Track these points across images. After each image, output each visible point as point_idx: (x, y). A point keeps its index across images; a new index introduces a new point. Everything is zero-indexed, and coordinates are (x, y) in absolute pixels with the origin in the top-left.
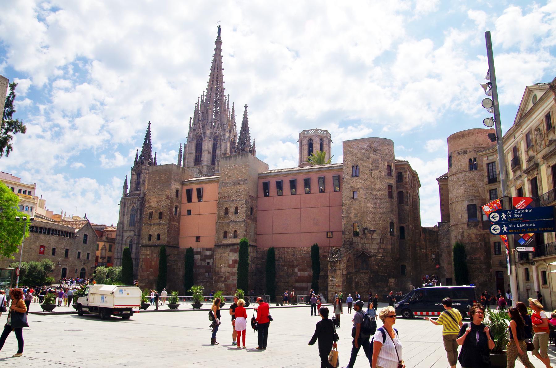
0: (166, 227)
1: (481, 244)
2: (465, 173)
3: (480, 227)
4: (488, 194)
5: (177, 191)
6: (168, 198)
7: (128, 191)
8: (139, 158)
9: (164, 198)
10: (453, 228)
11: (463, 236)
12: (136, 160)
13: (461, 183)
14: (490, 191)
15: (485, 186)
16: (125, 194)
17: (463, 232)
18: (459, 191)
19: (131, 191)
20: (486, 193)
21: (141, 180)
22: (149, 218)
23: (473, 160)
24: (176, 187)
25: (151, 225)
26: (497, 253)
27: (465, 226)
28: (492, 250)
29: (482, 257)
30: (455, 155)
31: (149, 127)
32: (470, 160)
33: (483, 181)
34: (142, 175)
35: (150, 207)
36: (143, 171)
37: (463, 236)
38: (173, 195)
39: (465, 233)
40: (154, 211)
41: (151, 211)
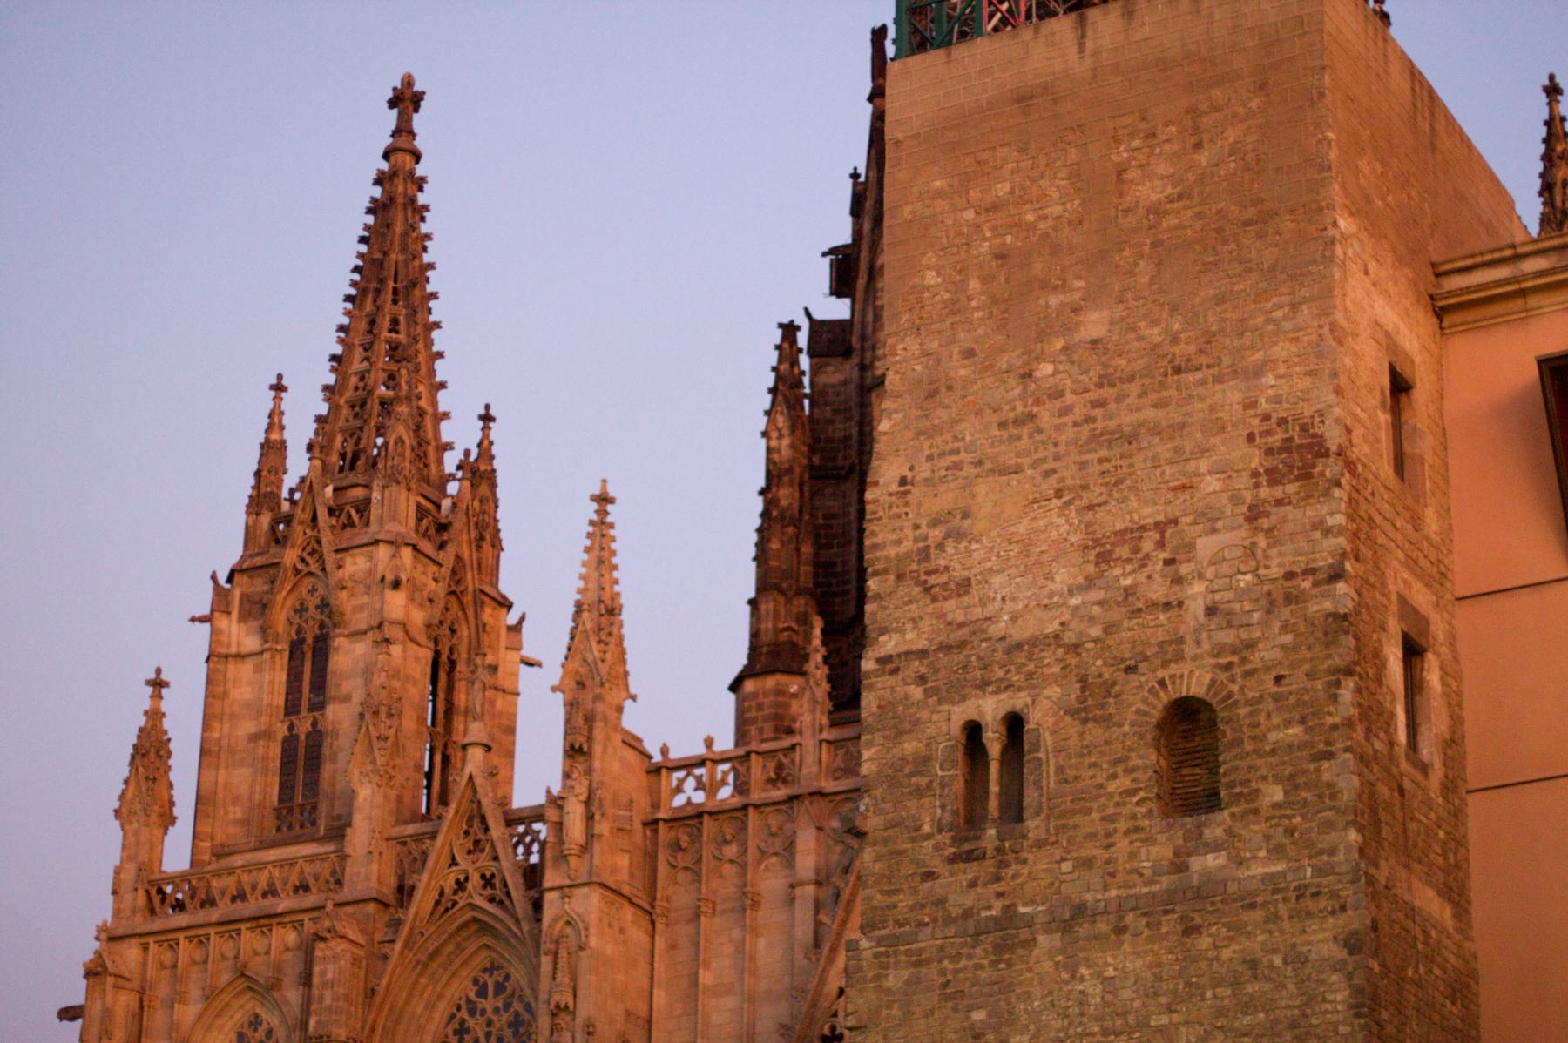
0: (1322, 940)
5: (1400, 386)
6: (1299, 456)
7: (176, 854)
8: (298, 465)
9: (1223, 471)
12: (262, 498)
16: (151, 897)
19: (211, 852)
21: (340, 715)
22: (972, 819)
24: (1388, 314)
25: (1007, 935)
31: (404, 130)
34: (348, 656)
35: (959, 658)
36: (354, 607)
38: (1358, 421)
40: (1044, 713)
41: (990, 709)
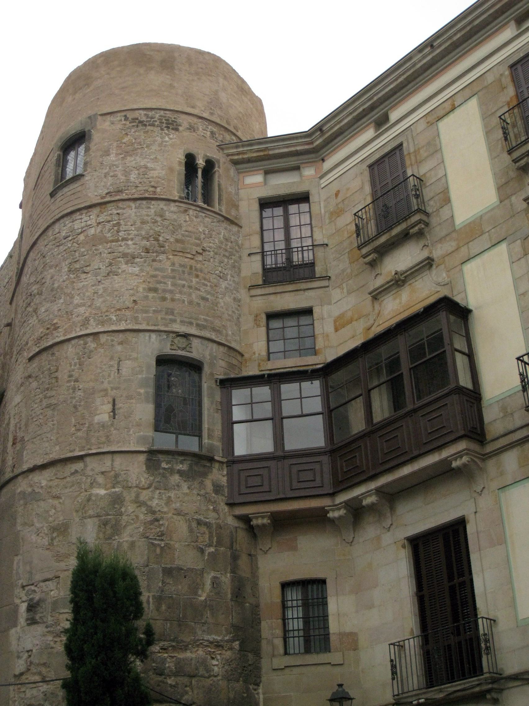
1: (215, 582)
2: (155, 206)
3: (217, 489)
4: (264, 329)
10: (42, 479)
11: (110, 526)
13: (131, 247)
14: (271, 316)
15: (243, 294)
17: (117, 500)
18: (117, 282)
20: (247, 323)
23: (201, 162)
26: (296, 643)
27: (136, 470)
28: (270, 629)
29: (217, 666)
30: (104, 133)
32: (190, 160)
33: (236, 268)
37: (110, 526)
39: (131, 508)
